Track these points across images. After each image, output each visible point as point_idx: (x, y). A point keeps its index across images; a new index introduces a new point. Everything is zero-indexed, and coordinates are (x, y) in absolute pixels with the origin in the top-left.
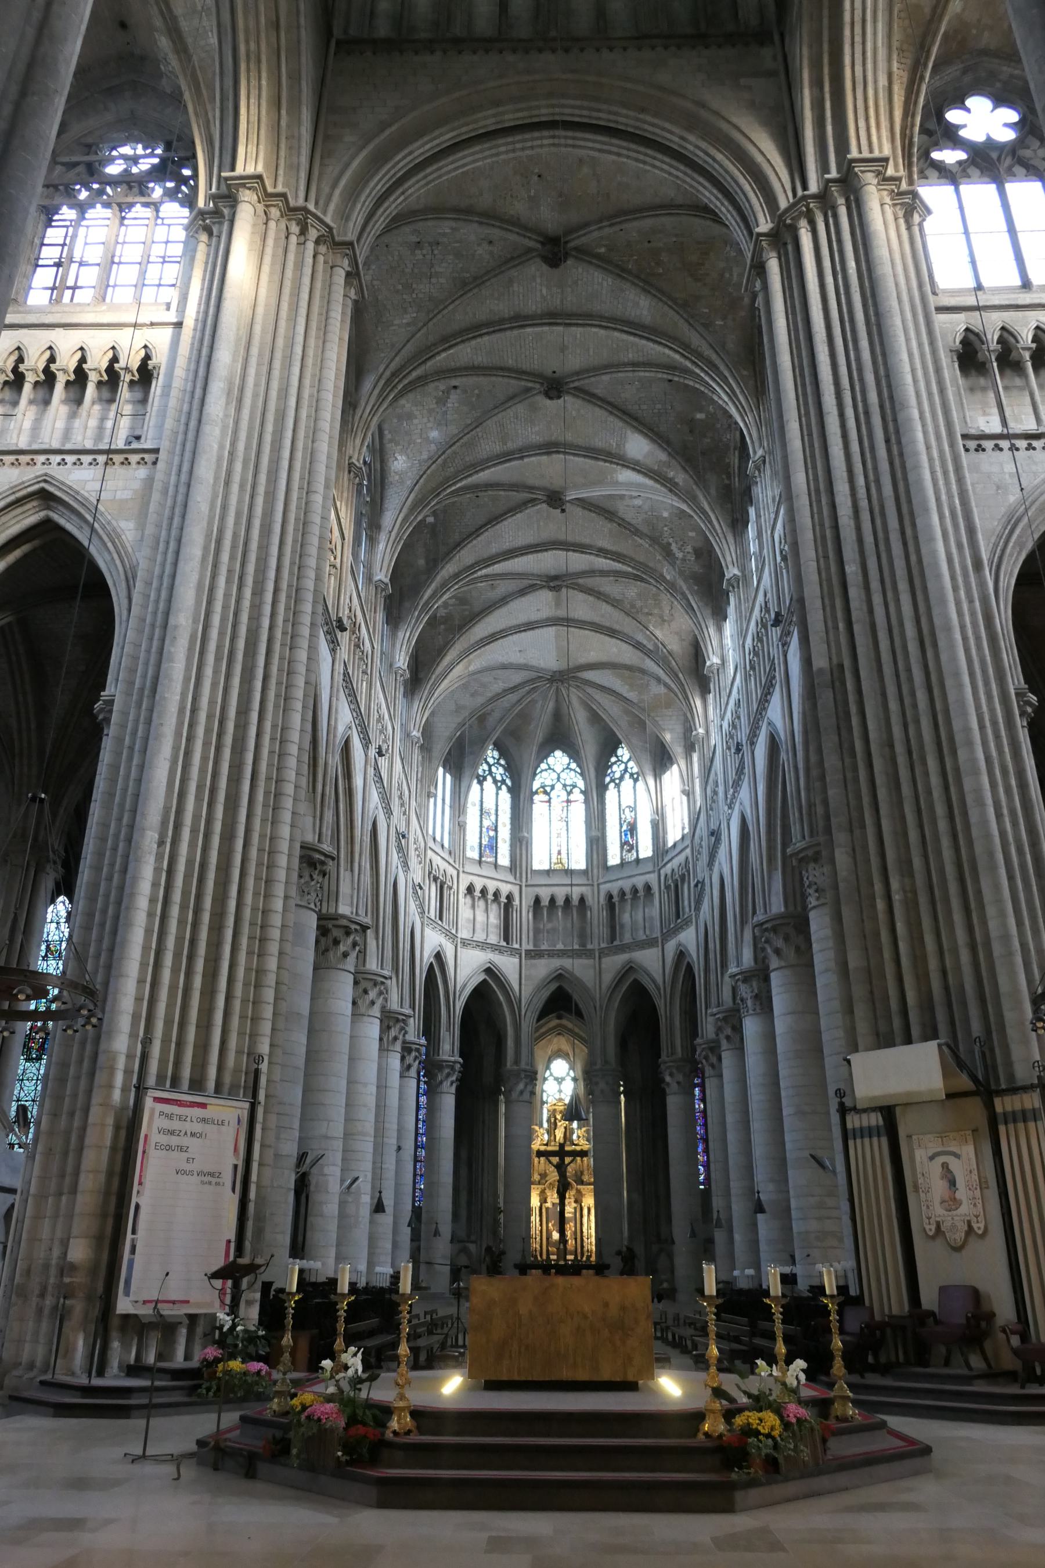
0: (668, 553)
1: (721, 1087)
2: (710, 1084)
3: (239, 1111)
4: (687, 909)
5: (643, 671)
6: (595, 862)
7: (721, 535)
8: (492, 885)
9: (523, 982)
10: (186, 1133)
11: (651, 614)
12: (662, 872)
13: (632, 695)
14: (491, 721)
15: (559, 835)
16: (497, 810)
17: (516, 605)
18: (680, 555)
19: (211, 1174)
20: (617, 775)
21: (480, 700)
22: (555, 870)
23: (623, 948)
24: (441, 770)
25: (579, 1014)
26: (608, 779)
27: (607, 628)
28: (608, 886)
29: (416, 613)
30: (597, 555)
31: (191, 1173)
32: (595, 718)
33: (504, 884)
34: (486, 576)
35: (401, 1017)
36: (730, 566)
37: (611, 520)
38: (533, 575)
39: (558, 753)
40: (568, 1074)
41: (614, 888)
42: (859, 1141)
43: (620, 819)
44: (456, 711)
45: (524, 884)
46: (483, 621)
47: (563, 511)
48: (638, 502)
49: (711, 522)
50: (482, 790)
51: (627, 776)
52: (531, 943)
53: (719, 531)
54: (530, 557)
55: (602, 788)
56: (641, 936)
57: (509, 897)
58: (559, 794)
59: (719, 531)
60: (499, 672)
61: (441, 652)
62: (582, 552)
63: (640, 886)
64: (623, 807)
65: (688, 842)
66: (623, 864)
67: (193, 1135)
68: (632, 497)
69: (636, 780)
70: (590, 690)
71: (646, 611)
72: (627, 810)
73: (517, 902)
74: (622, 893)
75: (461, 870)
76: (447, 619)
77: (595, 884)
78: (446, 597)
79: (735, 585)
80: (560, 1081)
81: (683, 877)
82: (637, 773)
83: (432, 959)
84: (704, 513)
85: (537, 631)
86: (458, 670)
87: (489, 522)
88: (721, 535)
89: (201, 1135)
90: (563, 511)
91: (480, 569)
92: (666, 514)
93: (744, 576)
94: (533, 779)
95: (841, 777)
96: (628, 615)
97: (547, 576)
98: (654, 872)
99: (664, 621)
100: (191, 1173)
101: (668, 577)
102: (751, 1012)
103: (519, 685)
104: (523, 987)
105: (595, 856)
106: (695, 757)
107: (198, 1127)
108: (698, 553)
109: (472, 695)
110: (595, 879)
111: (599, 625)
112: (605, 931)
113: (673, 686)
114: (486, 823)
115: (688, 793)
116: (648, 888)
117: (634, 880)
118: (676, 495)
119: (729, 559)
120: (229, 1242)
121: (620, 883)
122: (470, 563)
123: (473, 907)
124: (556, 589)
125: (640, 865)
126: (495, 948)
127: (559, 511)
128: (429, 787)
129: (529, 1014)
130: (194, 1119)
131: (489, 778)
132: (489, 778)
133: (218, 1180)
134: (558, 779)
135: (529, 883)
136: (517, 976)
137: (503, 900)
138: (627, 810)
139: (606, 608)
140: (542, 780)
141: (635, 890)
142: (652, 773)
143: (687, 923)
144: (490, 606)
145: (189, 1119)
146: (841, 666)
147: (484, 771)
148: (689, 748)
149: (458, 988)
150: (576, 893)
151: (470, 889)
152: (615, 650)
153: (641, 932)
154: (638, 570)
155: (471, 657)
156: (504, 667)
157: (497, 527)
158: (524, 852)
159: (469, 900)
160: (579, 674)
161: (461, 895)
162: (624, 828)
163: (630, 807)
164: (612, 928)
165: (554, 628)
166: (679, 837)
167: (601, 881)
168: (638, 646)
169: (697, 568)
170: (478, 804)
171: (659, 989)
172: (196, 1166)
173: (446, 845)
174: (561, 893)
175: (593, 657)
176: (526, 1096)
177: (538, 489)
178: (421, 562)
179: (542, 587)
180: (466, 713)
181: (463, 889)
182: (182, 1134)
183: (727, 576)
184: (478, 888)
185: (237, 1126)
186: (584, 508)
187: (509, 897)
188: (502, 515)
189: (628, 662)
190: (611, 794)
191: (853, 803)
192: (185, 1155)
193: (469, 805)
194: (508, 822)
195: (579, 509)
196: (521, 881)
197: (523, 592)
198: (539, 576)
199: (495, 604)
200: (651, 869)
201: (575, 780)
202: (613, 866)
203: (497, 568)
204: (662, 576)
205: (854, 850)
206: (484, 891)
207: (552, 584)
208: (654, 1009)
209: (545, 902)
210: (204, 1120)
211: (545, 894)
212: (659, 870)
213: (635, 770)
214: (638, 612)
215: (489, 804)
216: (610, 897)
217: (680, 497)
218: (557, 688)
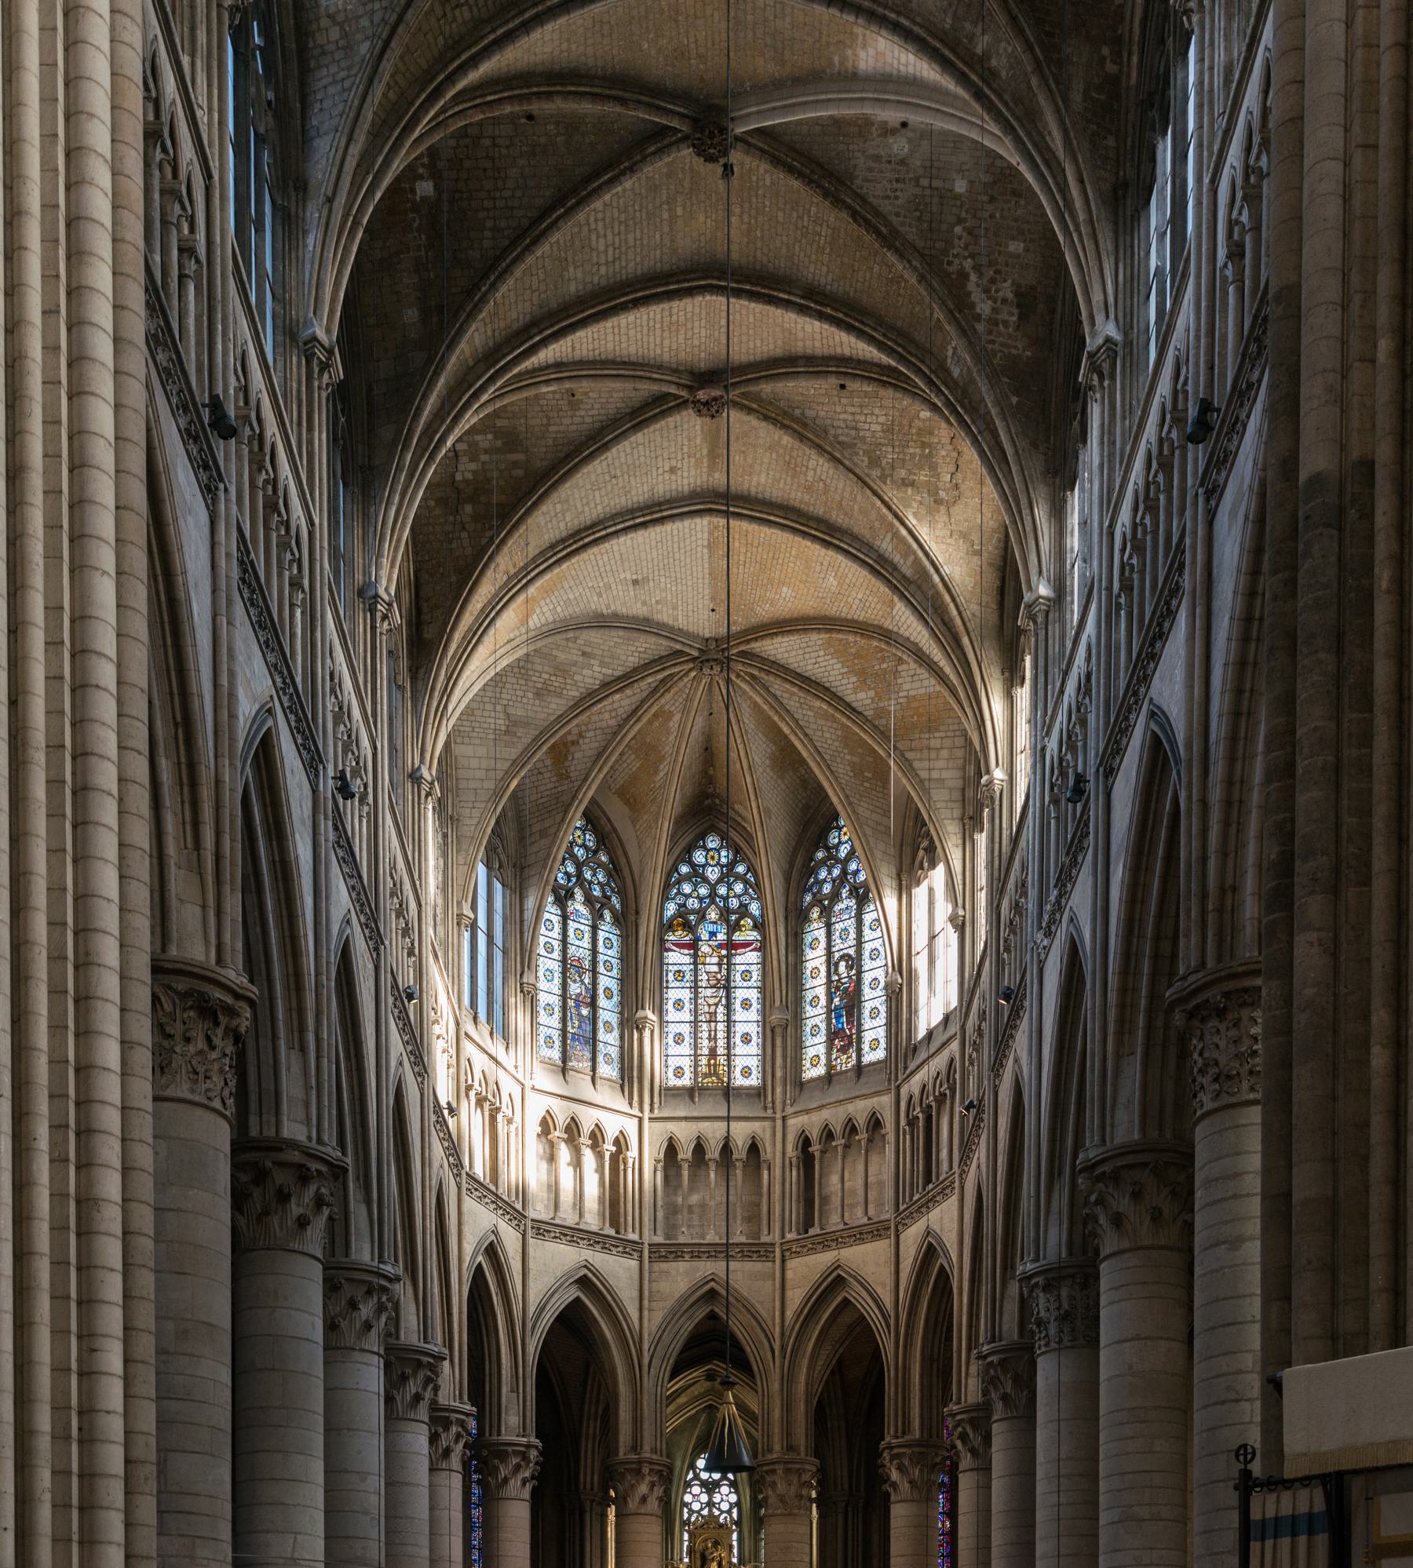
0: (959, 307)
1: (985, 1488)
2: (966, 1484)
4: (945, 1166)
5: (887, 635)
6: (779, 1074)
13: (862, 699)
14: (580, 758)
15: (712, 1019)
17: (621, 454)
18: (984, 308)
21: (556, 706)
22: (702, 1089)
24: (481, 870)
25: (743, 1365)
26: (808, 898)
28: (802, 1120)
30: (802, 310)
32: (787, 759)
34: (559, 365)
36: (1099, 318)
37: (837, 202)
38: (660, 367)
39: (712, 842)
44: (507, 732)
46: (555, 496)
47: (728, 170)
48: (899, 146)
49: (1064, 189)
50: (565, 918)
54: (655, 312)
55: (797, 919)
56: (858, 1217)
58: (713, 931)
59: (1082, 217)
60: (594, 636)
61: (466, 575)
62: (771, 300)
65: (954, 1028)
66: (830, 1078)
68: (887, 131)
70: (778, 686)
71: (903, 473)
76: (478, 489)
78: (470, 420)
81: (941, 1099)
82: (865, 884)
84: (1051, 160)
85: (669, 527)
86: (508, 620)
87: (560, 201)
90: (728, 170)
91: (544, 342)
92: (960, 186)
93: (1128, 343)
94: (665, 897)
97: (691, 373)
99: (938, 502)
101: (956, 372)
103: (635, 670)
105: (779, 1061)
106: (982, 839)
108: (1025, 301)
109: (538, 695)
112: (795, 1211)
113: (948, 670)
115: (960, 926)
118: (990, 108)
119: (1097, 297)
124: (709, 409)
127: (720, 170)
128: (459, 903)
132: (579, 895)
134: (713, 895)
139: (818, 466)
140: (680, 900)
141: (851, 1128)
142: (895, 884)
143: (944, 1192)
144: (568, 457)
147: (568, 875)
148: (971, 822)
150: (741, 1132)
152: (832, 581)
153: (859, 1211)
154: (890, 351)
155: (532, 590)
156: (602, 622)
157: (581, 216)
160: (757, 647)
164: (809, 1203)
168: (880, 567)
169: (1021, 348)
174: (714, 1132)
175: (787, 600)
177: (675, 96)
178: (411, 315)
179: (683, 404)
183: (1091, 344)
186: (776, 161)
187: (617, 1142)
188: (589, 179)
189: (860, 616)
195: (764, 166)
198: (675, 371)
199: (578, 448)
201: (746, 899)
203: (584, 342)
204: (942, 368)
207: (701, 395)
208: (876, 1354)
209: (685, 1153)
213: (862, 877)
214: (883, 478)
217: (999, 117)
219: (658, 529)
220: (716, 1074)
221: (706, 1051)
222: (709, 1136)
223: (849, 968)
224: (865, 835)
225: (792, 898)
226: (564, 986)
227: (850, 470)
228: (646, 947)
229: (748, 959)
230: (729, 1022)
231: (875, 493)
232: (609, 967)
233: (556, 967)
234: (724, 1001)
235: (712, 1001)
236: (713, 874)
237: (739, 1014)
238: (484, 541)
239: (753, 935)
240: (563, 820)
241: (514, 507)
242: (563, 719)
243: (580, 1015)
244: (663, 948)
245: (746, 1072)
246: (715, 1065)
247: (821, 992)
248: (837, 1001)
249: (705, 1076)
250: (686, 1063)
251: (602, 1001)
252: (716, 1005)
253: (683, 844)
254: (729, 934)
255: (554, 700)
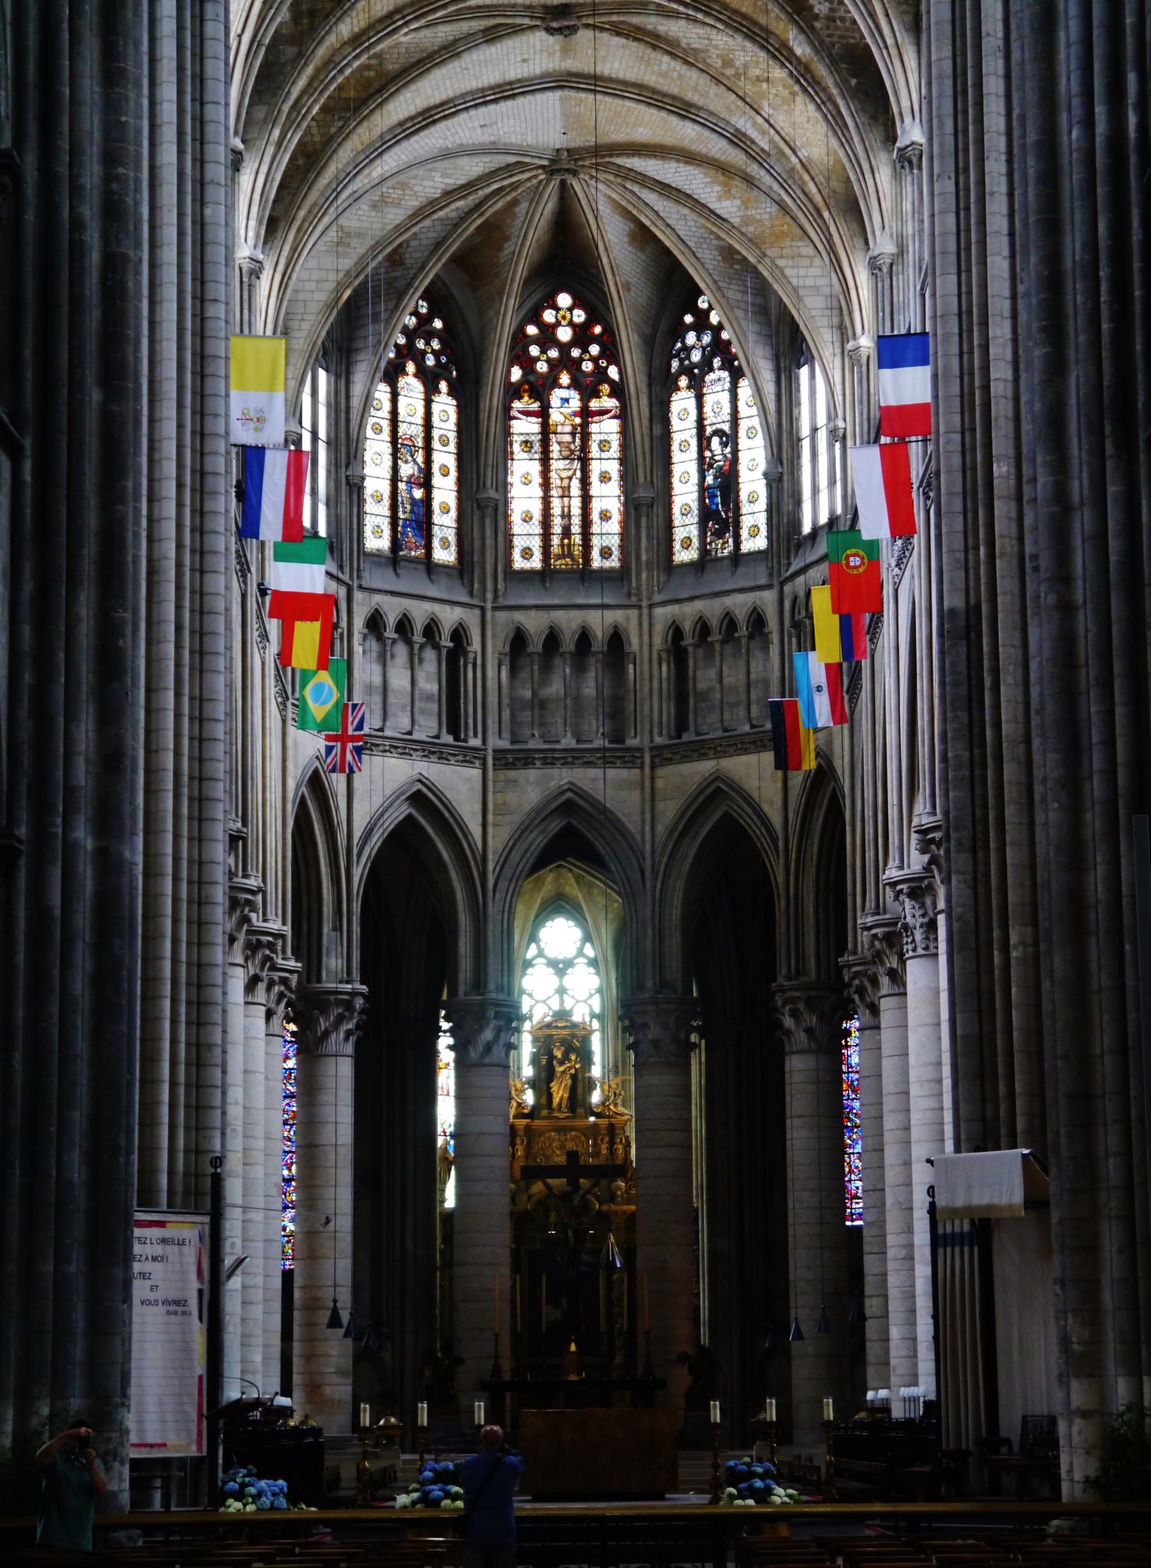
3: (199, 1227)
7: (894, 51)
8: (420, 612)
9: (490, 818)
10: (147, 1258)
11: (768, 80)
12: (787, 589)
15: (566, 493)
16: (428, 439)
19: (177, 1303)
20: (696, 356)
23: (700, 750)
27: (674, 98)
29: (277, 133)
31: (156, 1303)
33: (447, 608)
35: (265, 939)
40: (580, 953)
41: (687, 613)
42: (949, 1250)
43: (701, 458)
45: (489, 605)
51: (717, 362)
52: (506, 735)
53: (890, 41)
57: (459, 634)
63: (741, 616)
64: (709, 430)
67: (154, 1259)
69: (736, 375)
71: (757, 72)
72: (715, 441)
73: (476, 645)
74: (703, 627)
75: (356, 583)
77: (645, 604)
79: (915, 160)
80: (561, 967)
83: (304, 789)
85: (520, 100)
88: (894, 51)
89: (162, 1258)
95: (967, 773)
96: (719, 82)
98: (769, 587)
100: (156, 1303)
102: (920, 951)
104: (490, 829)
107: (158, 1250)
110: (644, 594)
111: (654, 91)
114: (407, 470)
116: (757, 620)
117: (728, 601)
120: (200, 1377)
121: (699, 605)
122: (385, 10)
123: (383, 660)
125: (741, 570)
126: (431, 750)
129: (503, 885)
130: (154, 1241)
131: (411, 367)
133: (185, 1309)
135: (502, 601)
136: (478, 807)
137: (446, 643)
138: (715, 441)
144: (420, 62)
145: (148, 1241)
146: (978, 606)
149: (356, 840)
151: (375, 623)
158: (489, 532)
159: (374, 645)
161: (357, 638)
162: (710, 480)
163: (719, 433)
165: (558, 94)
166: (823, 519)
167: (658, 598)
170: (386, 425)
171: (774, 840)
172: (158, 1295)
173: (322, 531)
176: (498, 1052)
180: (359, 248)
181: (359, 623)
182: (143, 1258)
184: (391, 619)
185: (199, 1245)
190: (682, 403)
191: (978, 812)
192: (148, 1283)
193: (369, 433)
194: (451, 461)
196: (484, 600)
197: (492, 35)
199: (431, 56)
200: (763, 581)
202: (683, 565)
205: (975, 879)
206: (404, 626)
209: (536, 645)
210: (164, 1241)
211: (534, 623)
212: (782, 584)
214: (737, 76)
215: (411, 427)
216: (676, 632)
218: (563, 183)
219: (509, 103)
220: (570, 555)
221: (557, 529)
222: (564, 626)
223: (724, 445)
224: (737, 319)
225: (656, 363)
226: (395, 469)
227: (703, 71)
228: (490, 424)
229: (607, 429)
230: (586, 499)
231: (729, 89)
232: (445, 442)
233: (387, 449)
234: (578, 474)
235: (564, 474)
236: (564, 334)
237: (596, 488)
238: (333, 130)
239: (610, 403)
240: (396, 307)
241: (364, 102)
242: (400, 229)
243: (412, 498)
244: (509, 418)
245: (606, 553)
246: (569, 545)
247: (693, 468)
248: (710, 480)
249: (559, 557)
250: (536, 544)
251: (437, 480)
252: (570, 478)
253: (529, 304)
254: (585, 400)
255: (393, 210)
